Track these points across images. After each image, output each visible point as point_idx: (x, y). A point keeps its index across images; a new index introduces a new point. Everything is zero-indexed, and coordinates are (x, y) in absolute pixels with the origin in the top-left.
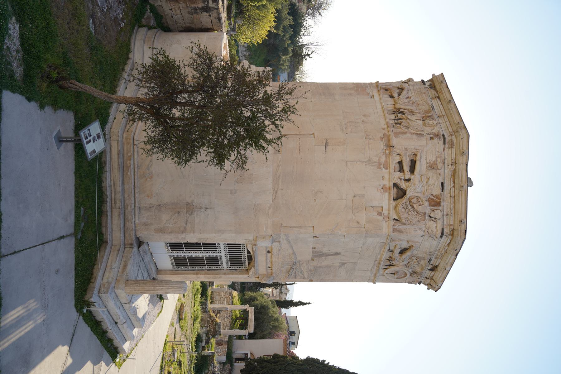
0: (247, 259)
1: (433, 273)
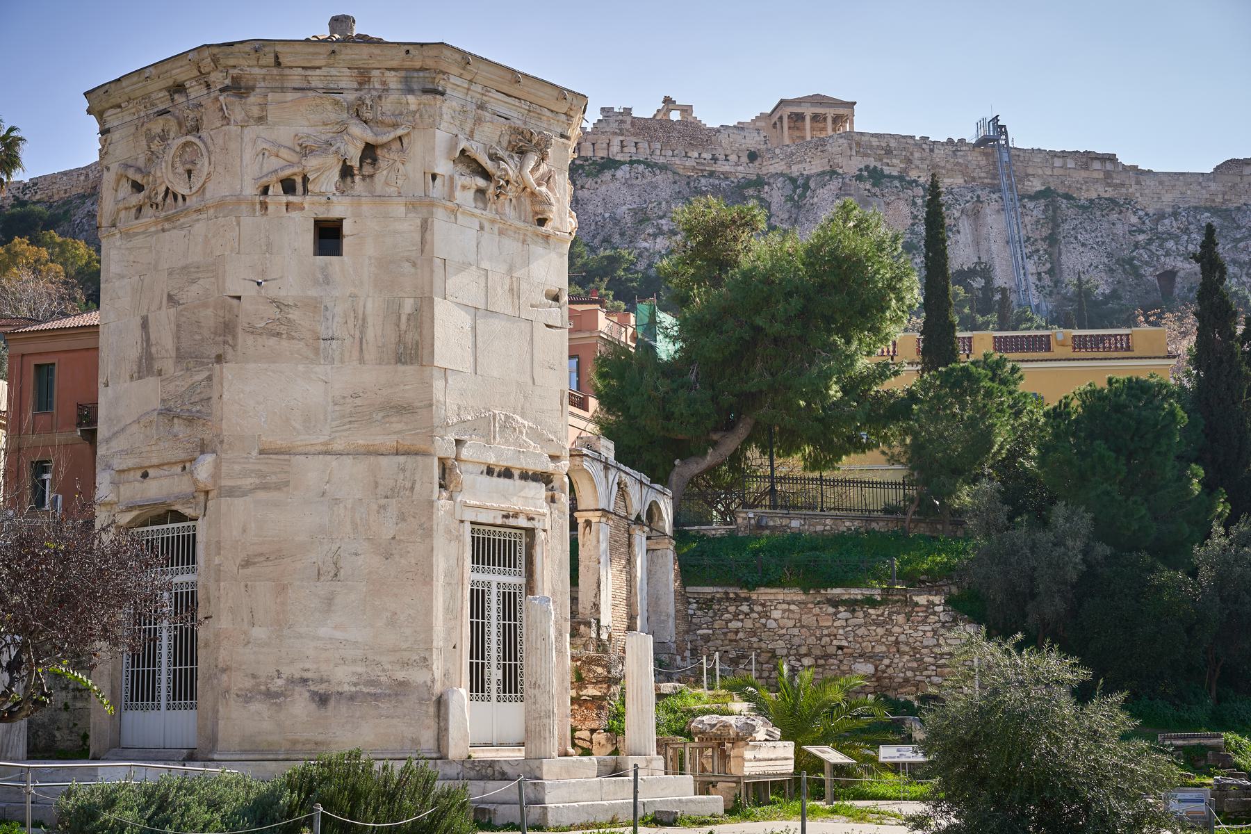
0: (180, 525)
1: (187, 85)
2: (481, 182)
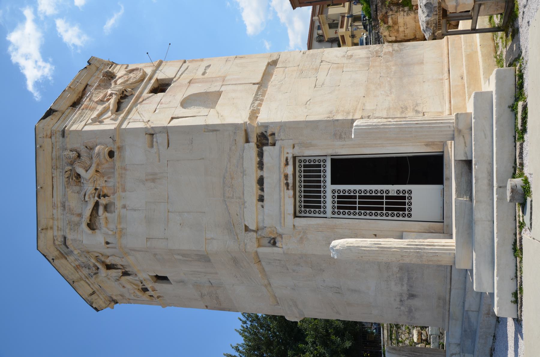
2: (101, 210)
